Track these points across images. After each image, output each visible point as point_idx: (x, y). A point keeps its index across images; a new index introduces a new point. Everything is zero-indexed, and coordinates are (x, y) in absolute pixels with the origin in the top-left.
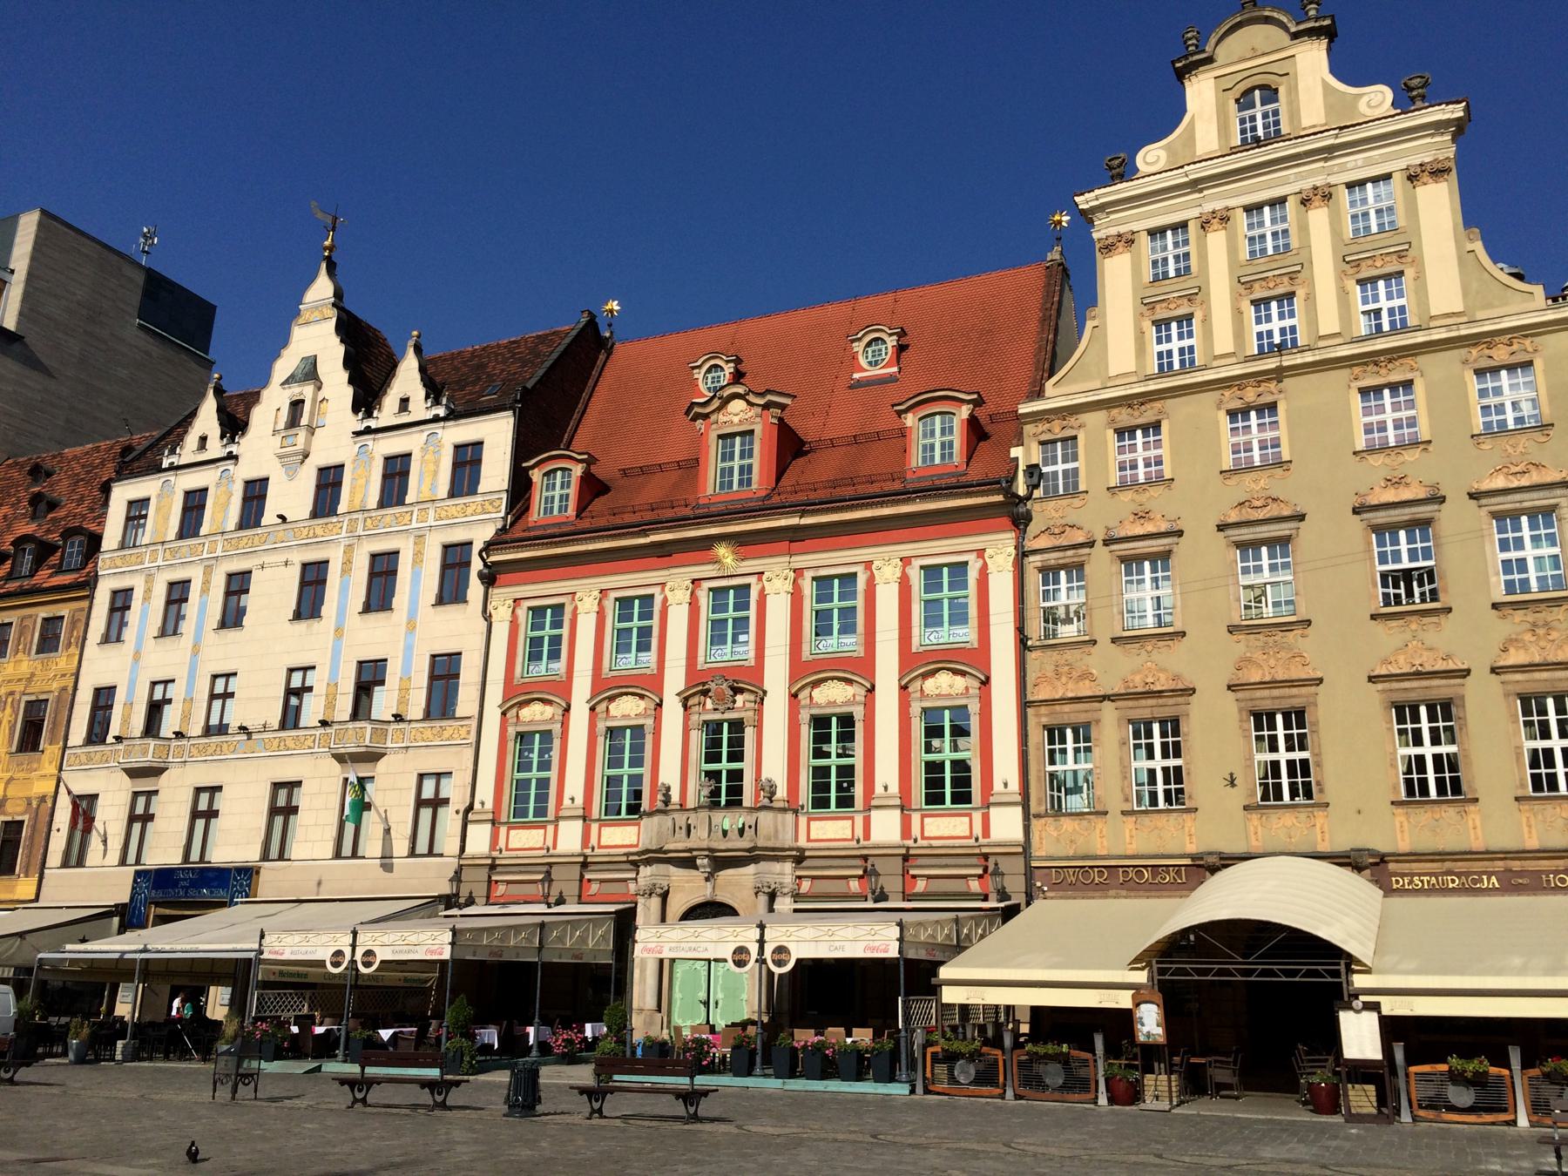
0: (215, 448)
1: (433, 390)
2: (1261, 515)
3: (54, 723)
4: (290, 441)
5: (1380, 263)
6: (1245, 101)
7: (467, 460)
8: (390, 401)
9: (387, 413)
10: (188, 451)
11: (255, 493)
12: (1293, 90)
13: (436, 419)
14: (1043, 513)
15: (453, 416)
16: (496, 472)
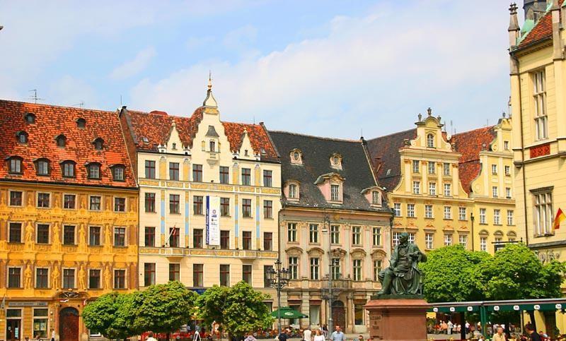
0: (180, 150)
1: (256, 150)
2: (430, 228)
3: (130, 237)
4: (213, 156)
5: (448, 183)
6: (428, 137)
7: (268, 175)
8: (242, 150)
9: (241, 155)
10: (169, 149)
11: (198, 170)
12: (436, 138)
13: (257, 161)
14: (396, 220)
15: (263, 160)
16: (276, 181)
